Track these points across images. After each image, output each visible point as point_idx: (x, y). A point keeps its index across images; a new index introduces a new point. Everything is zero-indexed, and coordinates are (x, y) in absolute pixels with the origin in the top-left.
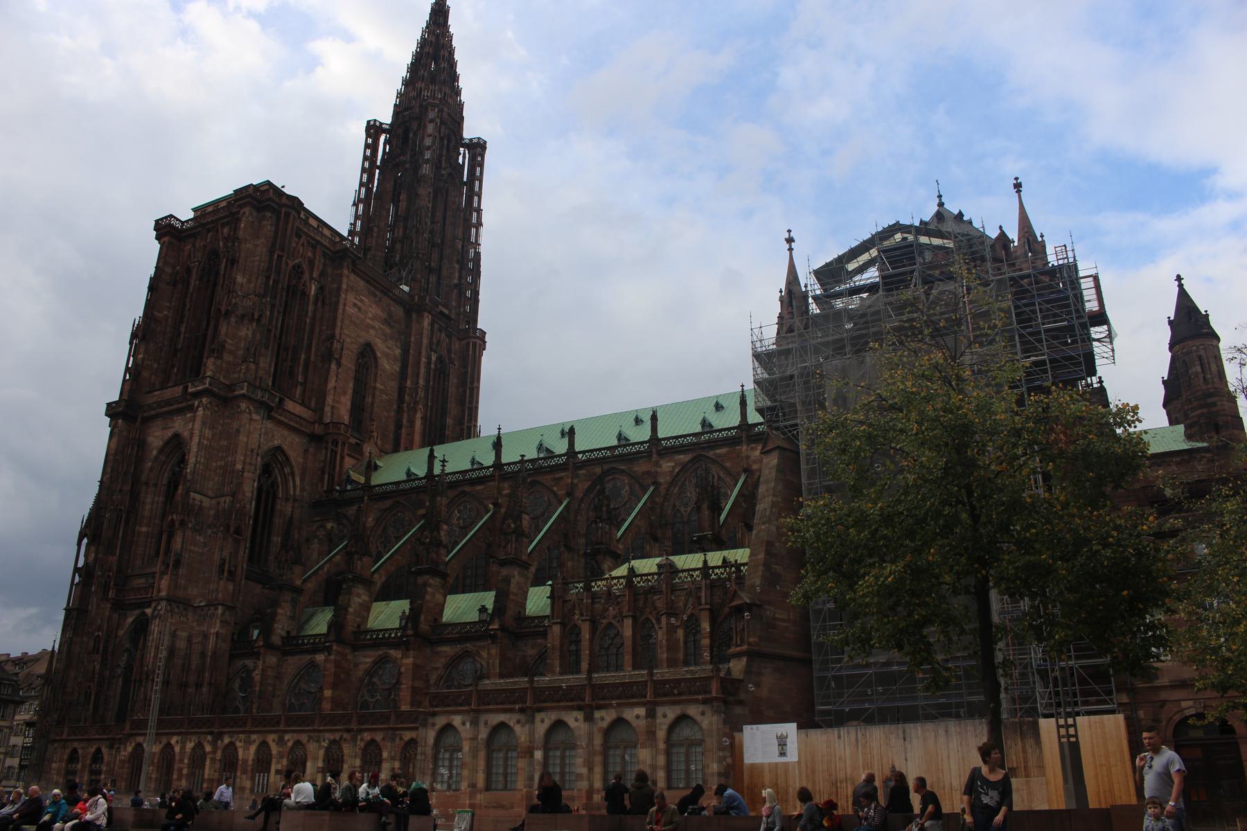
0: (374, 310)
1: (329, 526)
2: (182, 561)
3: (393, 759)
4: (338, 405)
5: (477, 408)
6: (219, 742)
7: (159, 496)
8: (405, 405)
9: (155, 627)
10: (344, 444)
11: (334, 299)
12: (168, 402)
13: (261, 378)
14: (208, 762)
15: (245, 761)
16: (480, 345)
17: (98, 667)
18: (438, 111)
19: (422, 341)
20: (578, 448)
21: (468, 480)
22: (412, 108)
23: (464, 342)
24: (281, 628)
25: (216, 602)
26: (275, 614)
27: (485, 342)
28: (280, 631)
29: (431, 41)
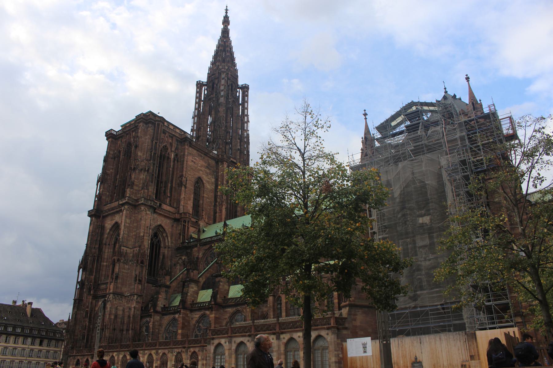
1: (183, 258)
2: (119, 276)
4: (187, 205)
7: (111, 249)
9: (108, 306)
11: (182, 159)
12: (113, 209)
13: (150, 195)
17: (87, 324)
18: (226, 74)
24: (161, 303)
25: (134, 294)
26: (157, 298)
28: (160, 305)
29: (222, 45)
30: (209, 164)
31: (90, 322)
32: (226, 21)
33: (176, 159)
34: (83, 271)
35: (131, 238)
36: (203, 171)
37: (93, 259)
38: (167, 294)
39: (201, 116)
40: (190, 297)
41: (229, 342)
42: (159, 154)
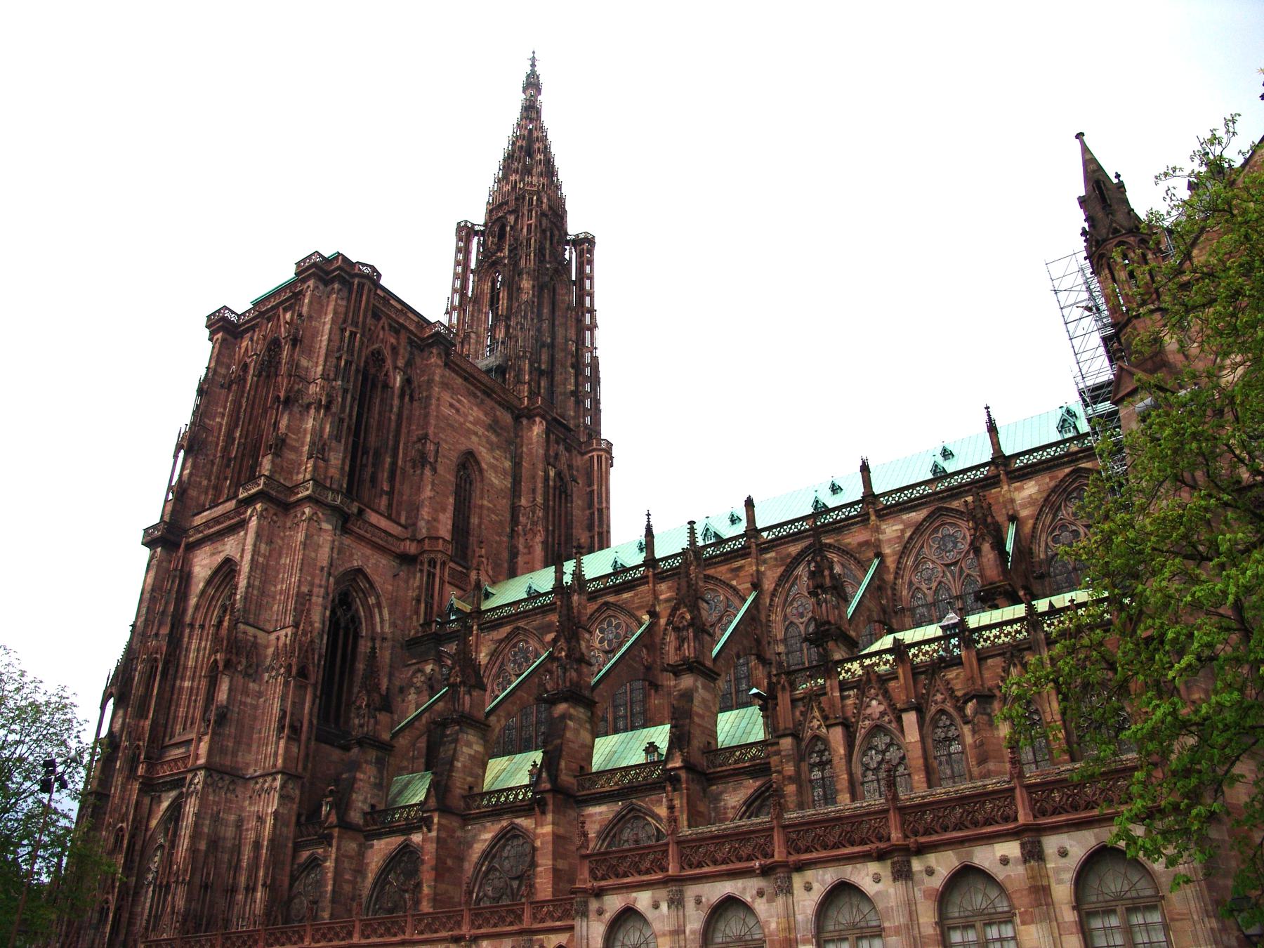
0: (476, 413)
1: (429, 668)
2: (229, 716)
4: (435, 524)
5: (608, 532)
7: (207, 640)
9: (191, 808)
10: (444, 564)
12: (216, 520)
13: (332, 478)
16: (606, 458)
20: (759, 525)
21: (610, 587)
22: (506, 203)
23: (587, 457)
24: (361, 801)
25: (274, 770)
26: (354, 780)
30: (496, 421)
31: (127, 868)
32: (533, 84)
33: (408, 392)
34: (116, 706)
35: (270, 600)
36: (479, 437)
38: (380, 771)
42: (362, 364)
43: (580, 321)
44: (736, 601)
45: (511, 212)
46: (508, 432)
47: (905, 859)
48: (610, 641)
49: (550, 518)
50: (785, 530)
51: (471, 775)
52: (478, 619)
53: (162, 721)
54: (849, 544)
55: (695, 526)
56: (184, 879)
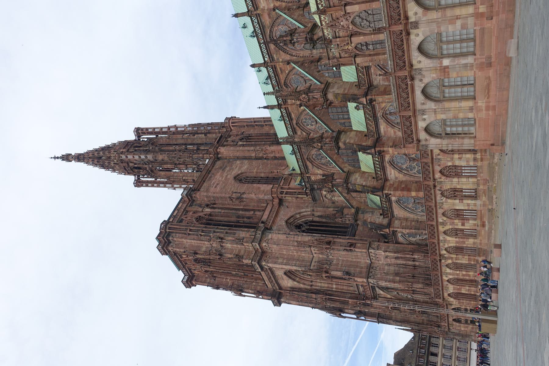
0: (218, 176)
1: (324, 193)
2: (347, 271)
3: (452, 159)
4: (265, 191)
5: (264, 118)
6: (445, 256)
8: (264, 156)
9: (383, 284)
10: (282, 188)
11: (212, 199)
12: (269, 279)
14: (459, 262)
15: (457, 242)
16: (233, 120)
18: (122, 154)
19: (232, 150)
22: (124, 167)
23: (232, 128)
24: (379, 219)
25: (368, 253)
27: (232, 117)
28: (380, 220)
29: (92, 160)
30: (221, 168)
32: (67, 158)
33: (212, 206)
34: (344, 313)
35: (300, 257)
36: (228, 174)
37: (329, 301)
38: (367, 212)
39: (171, 180)
40: (368, 182)
41: (423, 114)
42: (203, 226)
43: (174, 133)
44: (294, 71)
45: (128, 165)
46: (225, 162)
47: (410, 24)
48: (312, 122)
49: (259, 143)
50: (264, 51)
51: (368, 178)
52: (304, 174)
53: (349, 295)
54: (269, 22)
55: (266, 92)
56: (411, 285)
